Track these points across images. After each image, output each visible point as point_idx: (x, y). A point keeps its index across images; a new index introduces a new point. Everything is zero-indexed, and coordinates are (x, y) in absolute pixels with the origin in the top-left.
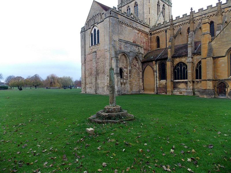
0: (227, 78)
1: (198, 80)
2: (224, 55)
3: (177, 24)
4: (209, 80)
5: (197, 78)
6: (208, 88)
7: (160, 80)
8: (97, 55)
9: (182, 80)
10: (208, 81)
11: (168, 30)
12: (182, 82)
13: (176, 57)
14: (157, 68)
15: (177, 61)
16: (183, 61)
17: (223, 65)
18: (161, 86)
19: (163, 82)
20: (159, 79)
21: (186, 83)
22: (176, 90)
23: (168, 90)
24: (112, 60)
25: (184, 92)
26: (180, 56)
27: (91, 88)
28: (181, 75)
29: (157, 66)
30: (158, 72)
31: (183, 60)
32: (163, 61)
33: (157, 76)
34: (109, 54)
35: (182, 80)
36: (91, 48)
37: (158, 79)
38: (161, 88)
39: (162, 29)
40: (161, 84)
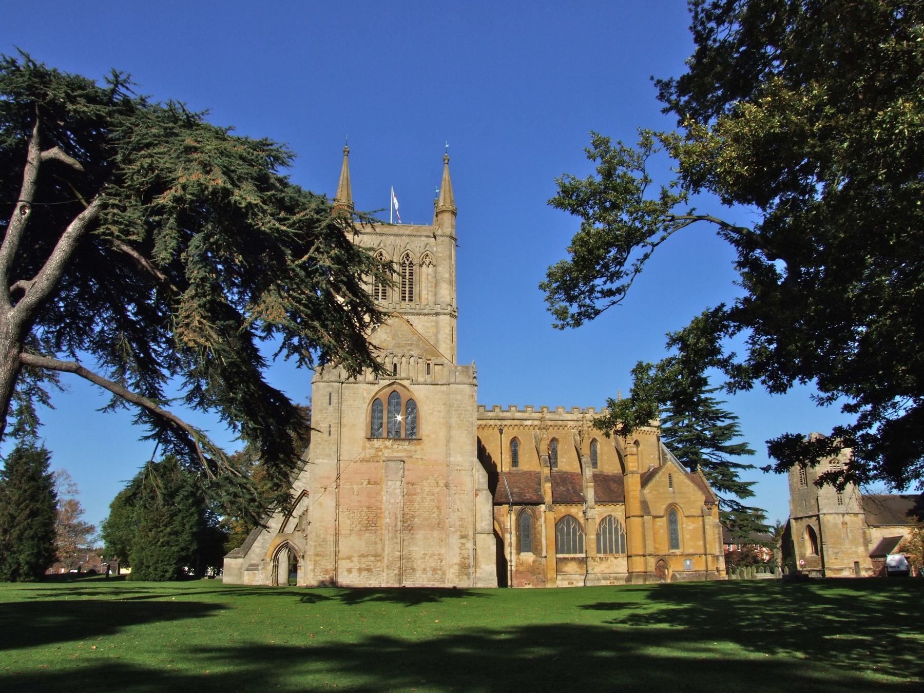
0: (666, 552)
1: (602, 555)
2: (662, 514)
3: (529, 423)
4: (650, 555)
5: (599, 551)
6: (649, 569)
7: (518, 553)
8: (406, 473)
9: (572, 556)
10: (648, 558)
11: (506, 429)
12: (573, 559)
13: (560, 503)
14: (513, 523)
15: (562, 510)
16: (573, 514)
17: (662, 531)
18: (521, 569)
19: (528, 557)
20: (516, 549)
21: (583, 562)
22: (559, 577)
23: (549, 576)
24: (477, 495)
25: (577, 580)
26: (569, 502)
27: (369, 570)
28: (569, 543)
29: (514, 517)
30: (514, 532)
31: (576, 511)
32: (529, 509)
33: (511, 543)
34: (470, 479)
35: (572, 556)
36: (377, 443)
37: (514, 551)
38: (521, 573)
39: (491, 422)
40: (522, 564)
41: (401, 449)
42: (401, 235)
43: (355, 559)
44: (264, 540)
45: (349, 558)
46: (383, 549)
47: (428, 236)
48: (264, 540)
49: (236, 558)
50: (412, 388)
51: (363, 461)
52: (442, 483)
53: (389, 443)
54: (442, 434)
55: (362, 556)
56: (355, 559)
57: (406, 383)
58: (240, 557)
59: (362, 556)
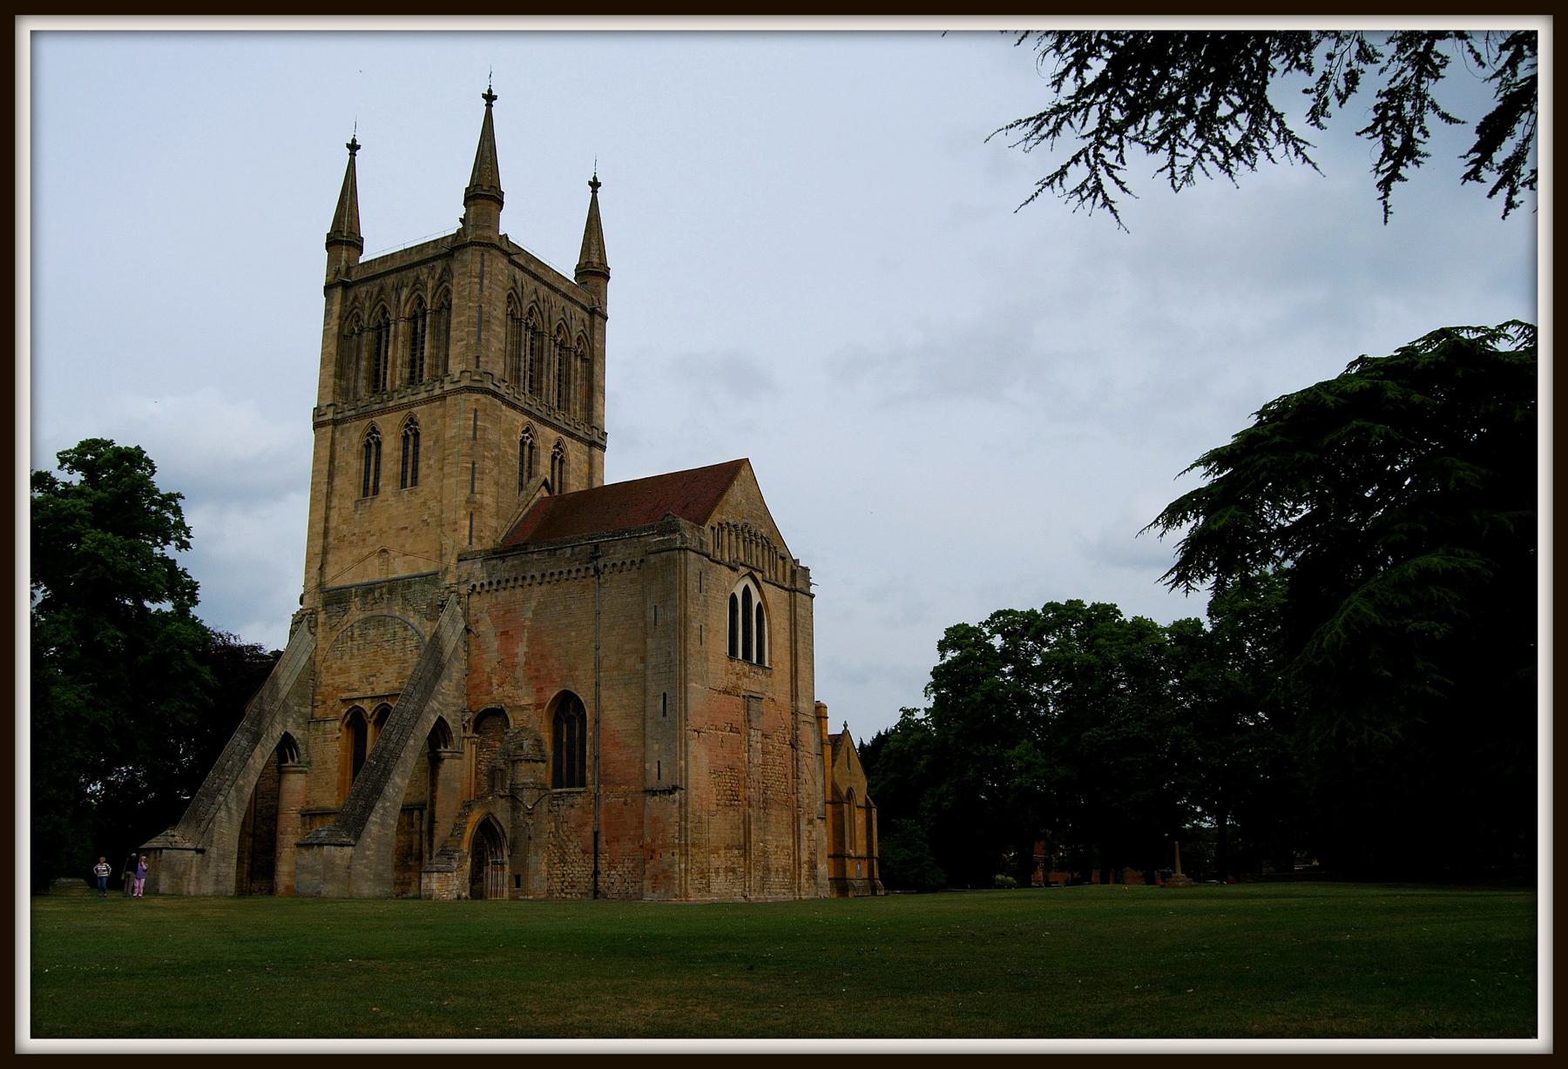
27: (733, 870)
41: (752, 683)
42: (556, 290)
43: (722, 852)
44: (384, 808)
45: (716, 851)
46: (747, 833)
47: (583, 308)
48: (384, 808)
49: (342, 845)
50: (764, 586)
51: (725, 692)
52: (788, 737)
53: (747, 668)
54: (788, 664)
55: (728, 848)
56: (722, 852)
57: (759, 576)
58: (349, 845)
59: (728, 848)
